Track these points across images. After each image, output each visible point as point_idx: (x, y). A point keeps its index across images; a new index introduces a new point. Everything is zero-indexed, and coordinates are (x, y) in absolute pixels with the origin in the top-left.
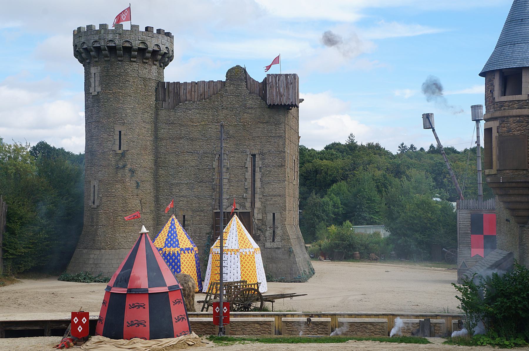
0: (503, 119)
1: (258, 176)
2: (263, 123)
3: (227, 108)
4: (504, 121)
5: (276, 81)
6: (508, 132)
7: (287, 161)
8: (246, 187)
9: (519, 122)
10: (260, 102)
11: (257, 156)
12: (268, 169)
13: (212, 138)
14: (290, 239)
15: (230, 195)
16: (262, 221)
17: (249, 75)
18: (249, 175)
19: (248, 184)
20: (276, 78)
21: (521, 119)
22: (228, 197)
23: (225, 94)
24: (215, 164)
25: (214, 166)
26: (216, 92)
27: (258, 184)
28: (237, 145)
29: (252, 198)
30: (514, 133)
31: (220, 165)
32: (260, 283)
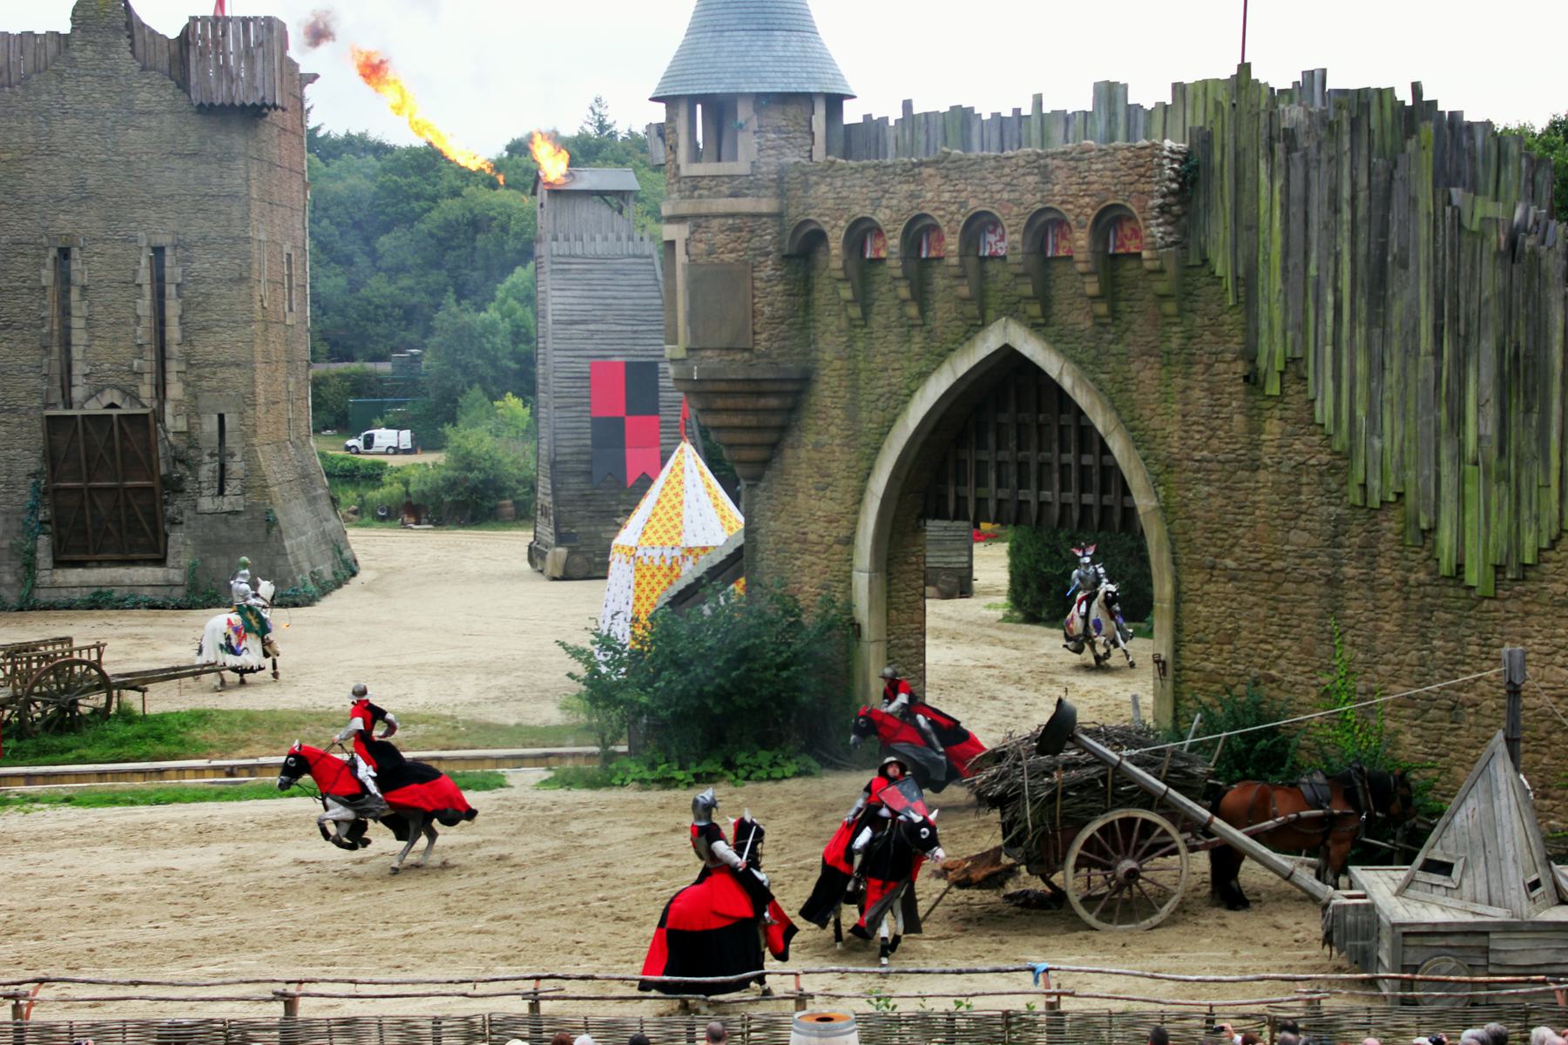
0: (700, 221)
1: (173, 309)
2: (181, 155)
3: (76, 113)
4: (699, 226)
5: (215, 35)
6: (709, 254)
7: (256, 266)
8: (139, 342)
9: (732, 229)
10: (173, 94)
11: (168, 252)
12: (203, 289)
13: (37, 199)
14: (267, 487)
15: (94, 365)
16: (189, 437)
17: (138, 18)
18: (145, 306)
19: (144, 333)
20: (214, 28)
21: (738, 221)
22: (88, 371)
23: (69, 70)
24: (47, 276)
25: (44, 282)
26: (42, 66)
27: (173, 332)
28: (108, 219)
29: (157, 373)
30: (722, 256)
31: (64, 280)
32: (104, 645)
